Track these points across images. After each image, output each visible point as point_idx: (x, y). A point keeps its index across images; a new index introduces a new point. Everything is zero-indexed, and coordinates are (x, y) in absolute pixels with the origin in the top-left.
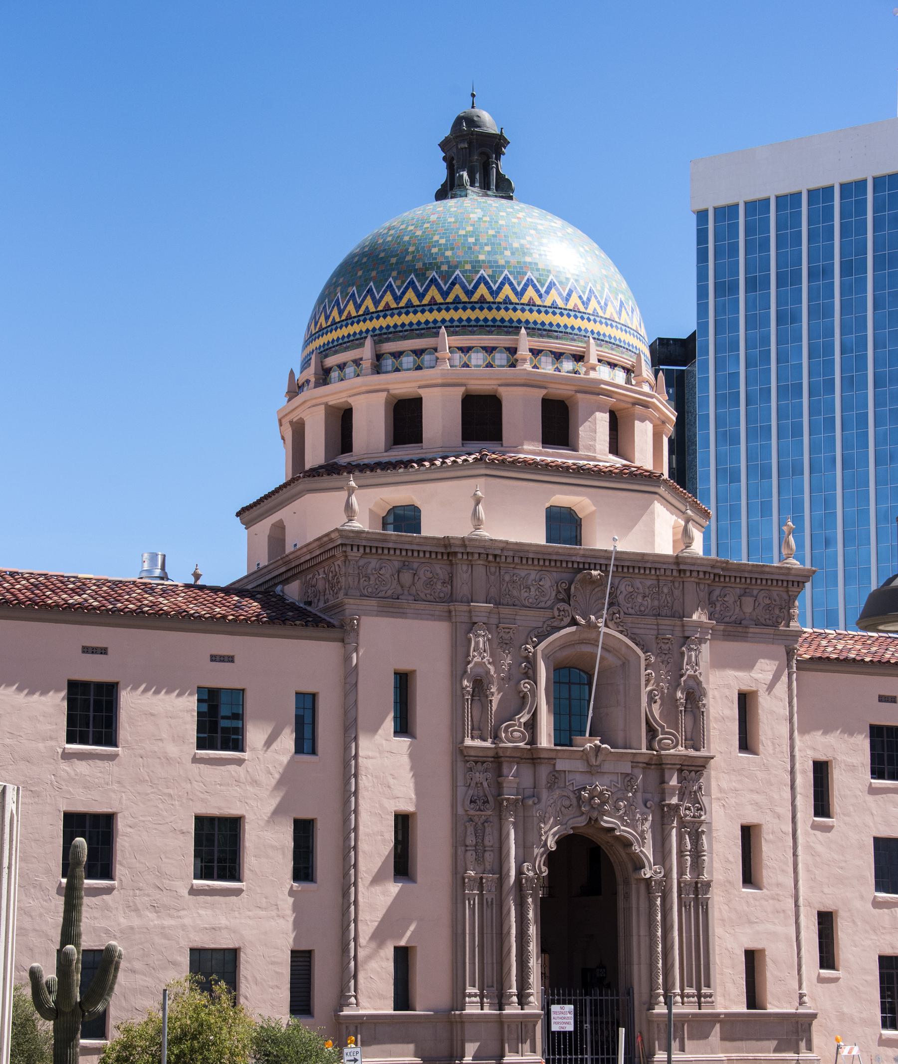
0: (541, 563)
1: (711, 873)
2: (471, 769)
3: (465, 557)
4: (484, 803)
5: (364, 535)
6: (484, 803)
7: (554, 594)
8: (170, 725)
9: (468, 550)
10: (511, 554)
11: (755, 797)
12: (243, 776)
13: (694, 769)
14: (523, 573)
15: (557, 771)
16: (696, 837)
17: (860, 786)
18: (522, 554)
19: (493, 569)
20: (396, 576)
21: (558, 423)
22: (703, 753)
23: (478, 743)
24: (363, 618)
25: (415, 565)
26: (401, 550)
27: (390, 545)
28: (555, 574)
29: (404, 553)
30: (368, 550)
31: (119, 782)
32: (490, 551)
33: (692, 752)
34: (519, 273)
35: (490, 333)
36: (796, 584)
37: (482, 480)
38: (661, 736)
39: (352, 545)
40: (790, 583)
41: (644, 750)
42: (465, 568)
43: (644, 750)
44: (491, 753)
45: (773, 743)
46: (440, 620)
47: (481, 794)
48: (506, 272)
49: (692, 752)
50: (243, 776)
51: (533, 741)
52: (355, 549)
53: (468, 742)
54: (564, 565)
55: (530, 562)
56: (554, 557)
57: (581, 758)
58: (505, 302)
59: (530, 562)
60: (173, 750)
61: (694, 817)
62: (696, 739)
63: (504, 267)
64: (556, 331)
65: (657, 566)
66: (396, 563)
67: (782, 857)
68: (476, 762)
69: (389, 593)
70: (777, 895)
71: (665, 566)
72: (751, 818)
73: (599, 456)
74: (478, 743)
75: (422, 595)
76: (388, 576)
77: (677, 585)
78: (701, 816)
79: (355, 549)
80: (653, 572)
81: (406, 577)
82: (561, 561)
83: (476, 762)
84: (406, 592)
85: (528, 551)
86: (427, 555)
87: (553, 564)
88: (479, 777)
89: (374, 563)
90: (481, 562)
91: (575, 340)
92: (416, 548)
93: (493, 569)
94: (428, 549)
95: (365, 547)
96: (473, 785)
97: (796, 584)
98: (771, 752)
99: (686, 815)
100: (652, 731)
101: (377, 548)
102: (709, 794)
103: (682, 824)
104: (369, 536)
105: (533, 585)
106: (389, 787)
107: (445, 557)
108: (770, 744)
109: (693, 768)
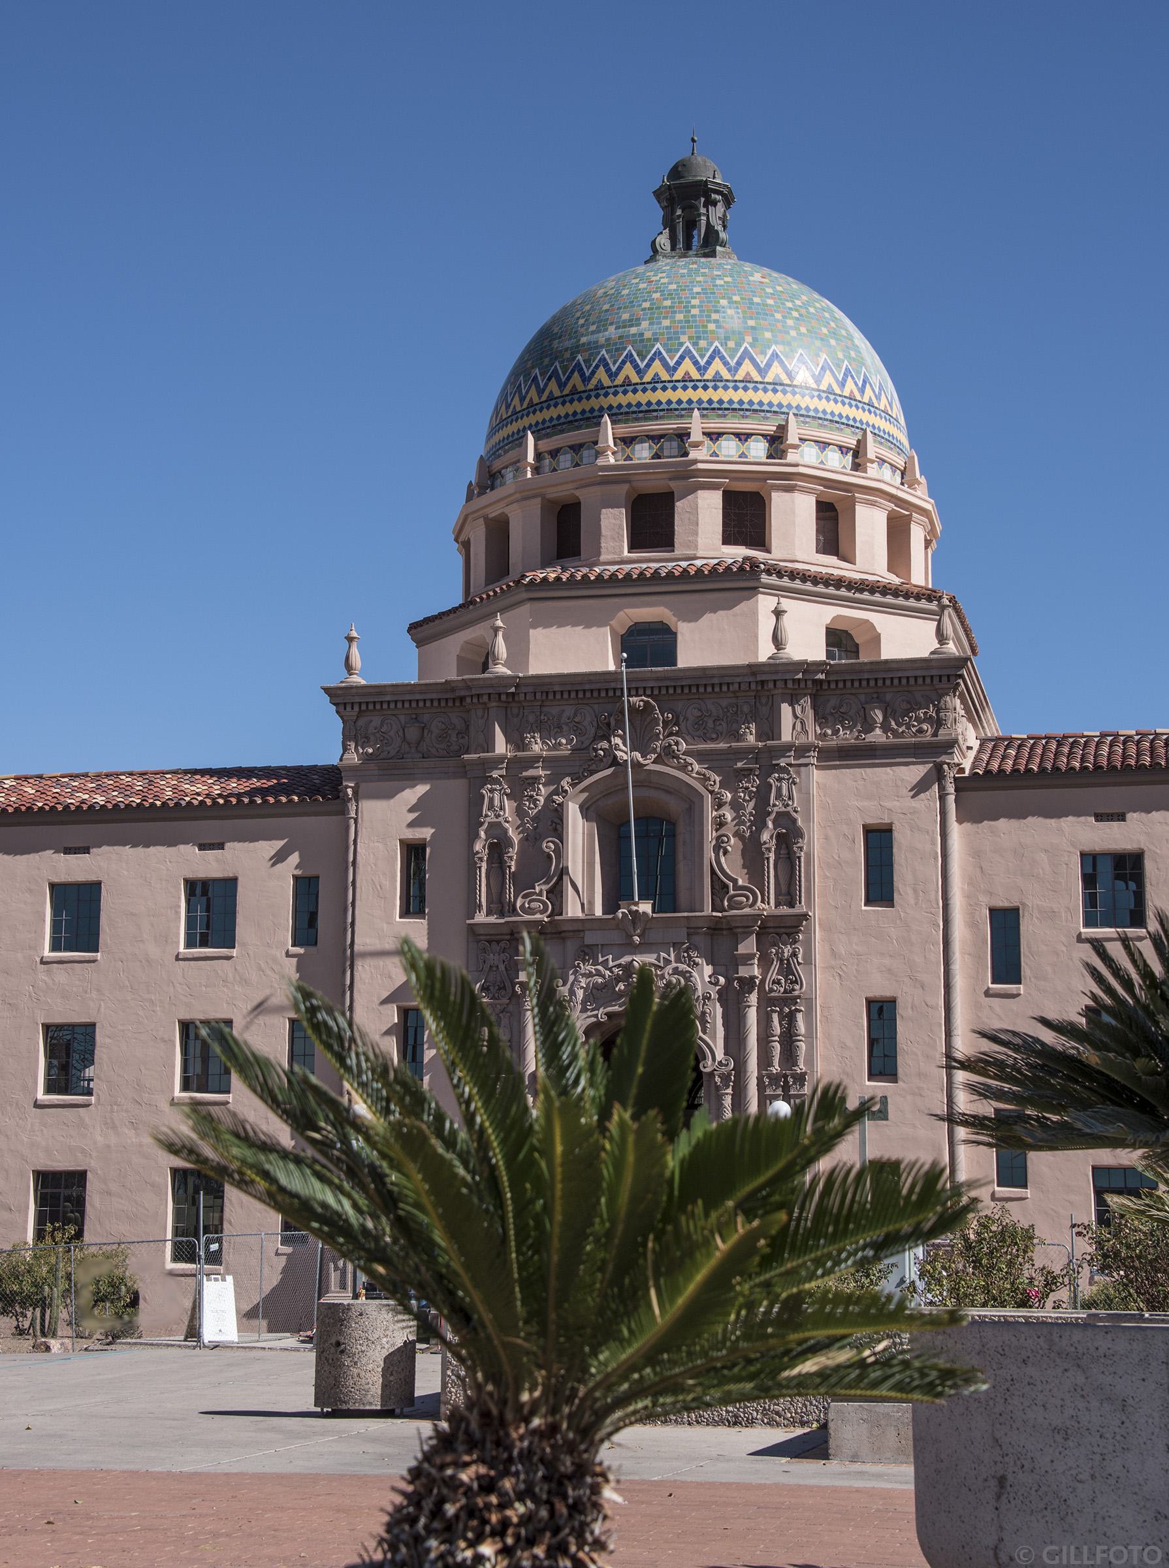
0: (573, 695)
1: (810, 1061)
2: (484, 950)
3: (475, 700)
4: (500, 989)
5: (354, 691)
6: (500, 989)
7: (593, 730)
8: (152, 925)
9: (474, 692)
10: (530, 689)
11: (887, 961)
12: (230, 975)
13: (785, 930)
14: (555, 711)
15: (588, 946)
16: (789, 1020)
17: (1064, 939)
18: (545, 689)
19: (515, 711)
20: (401, 733)
21: (653, 521)
22: (797, 910)
23: (492, 919)
24: (363, 786)
25: (426, 718)
26: (403, 702)
27: (388, 698)
28: (596, 706)
29: (407, 705)
30: (364, 707)
31: (98, 990)
32: (501, 690)
33: (785, 910)
34: (617, 350)
35: (579, 428)
36: (945, 679)
37: (527, 607)
38: (732, 892)
39: (345, 704)
40: (936, 680)
41: (708, 910)
42: (480, 713)
43: (708, 910)
44: (506, 930)
45: (915, 891)
46: (455, 778)
47: (499, 979)
48: (604, 352)
49: (785, 910)
50: (230, 975)
51: (559, 909)
52: (349, 708)
53: (481, 918)
54: (603, 694)
55: (558, 696)
56: (587, 687)
57: (618, 928)
58: (596, 388)
59: (558, 696)
60: (153, 951)
61: (785, 992)
62: (788, 895)
63: (602, 346)
64: (656, 411)
65: (727, 680)
66: (402, 718)
67: (927, 1039)
68: (489, 942)
69: (393, 753)
70: (919, 1088)
71: (738, 679)
72: (881, 990)
73: (700, 553)
74: (492, 919)
75: (433, 751)
76: (392, 733)
77: (764, 700)
78: (794, 990)
79: (349, 708)
80: (725, 688)
81: (412, 733)
82: (599, 690)
83: (489, 942)
84: (413, 750)
85: (551, 684)
86: (436, 704)
87: (588, 695)
88: (493, 959)
89: (376, 721)
90: (494, 704)
91: (682, 416)
92: (418, 697)
93: (515, 711)
94: (434, 696)
95: (360, 703)
96: (486, 968)
97: (945, 679)
98: (912, 901)
99: (771, 990)
100: (720, 888)
101: (374, 703)
102: (809, 961)
103: (767, 1002)
104: (360, 691)
105: (567, 724)
106: (390, 977)
107: (458, 704)
108: (910, 891)
109: (783, 930)
